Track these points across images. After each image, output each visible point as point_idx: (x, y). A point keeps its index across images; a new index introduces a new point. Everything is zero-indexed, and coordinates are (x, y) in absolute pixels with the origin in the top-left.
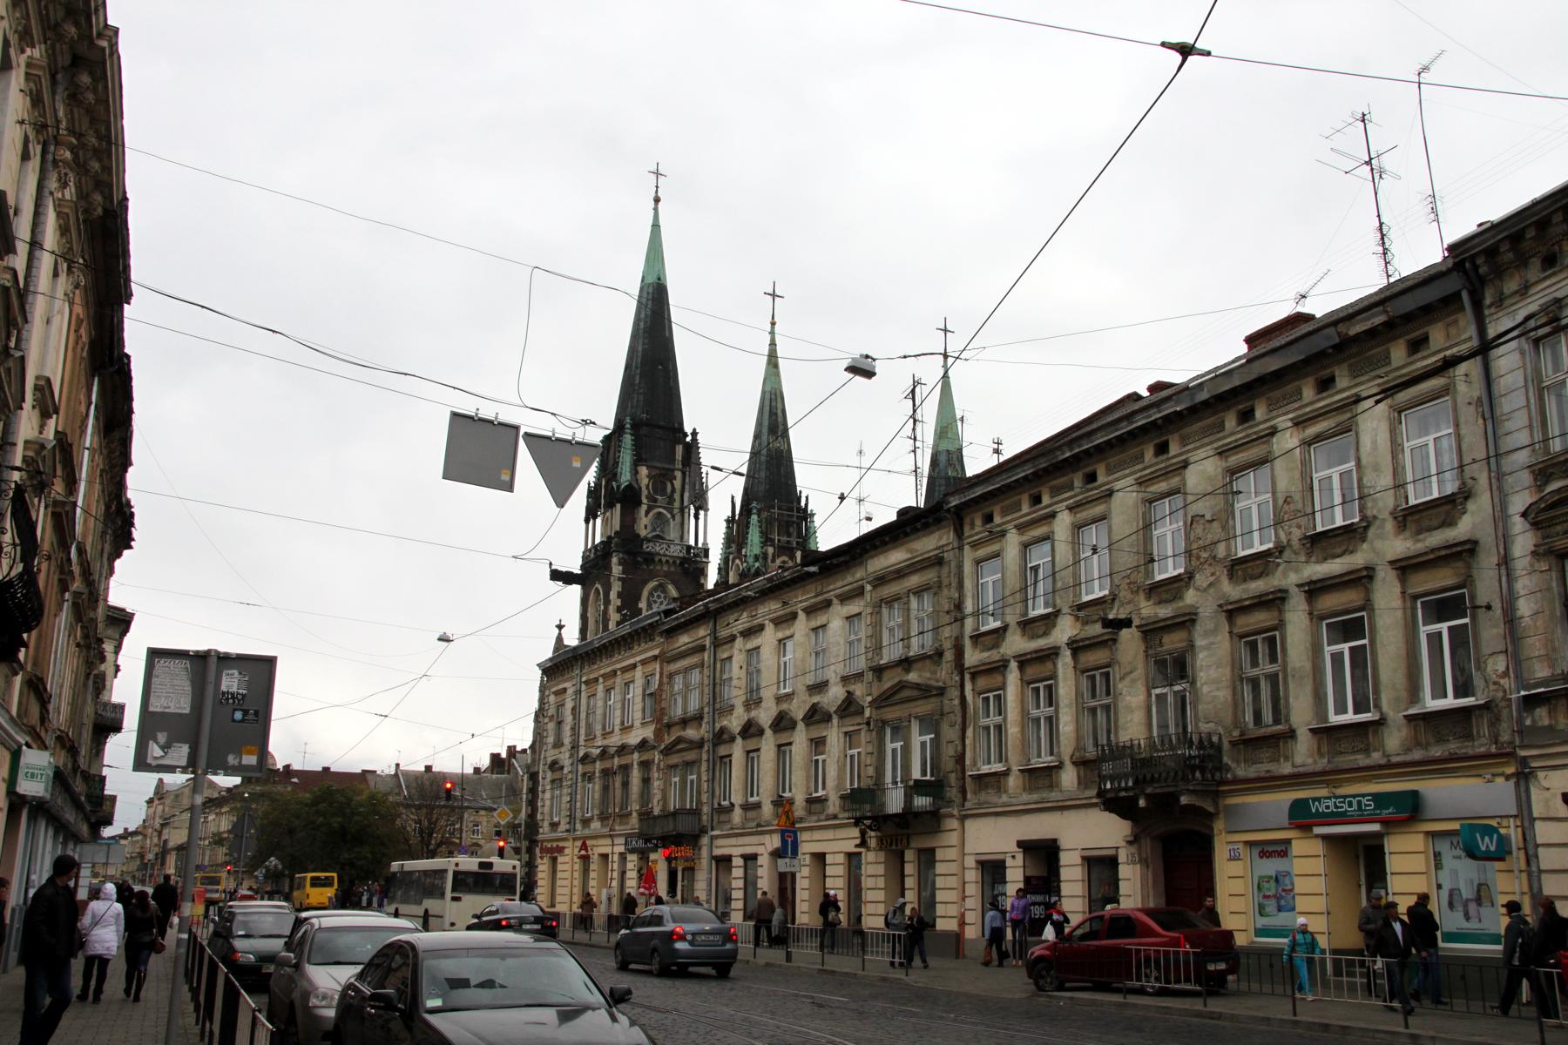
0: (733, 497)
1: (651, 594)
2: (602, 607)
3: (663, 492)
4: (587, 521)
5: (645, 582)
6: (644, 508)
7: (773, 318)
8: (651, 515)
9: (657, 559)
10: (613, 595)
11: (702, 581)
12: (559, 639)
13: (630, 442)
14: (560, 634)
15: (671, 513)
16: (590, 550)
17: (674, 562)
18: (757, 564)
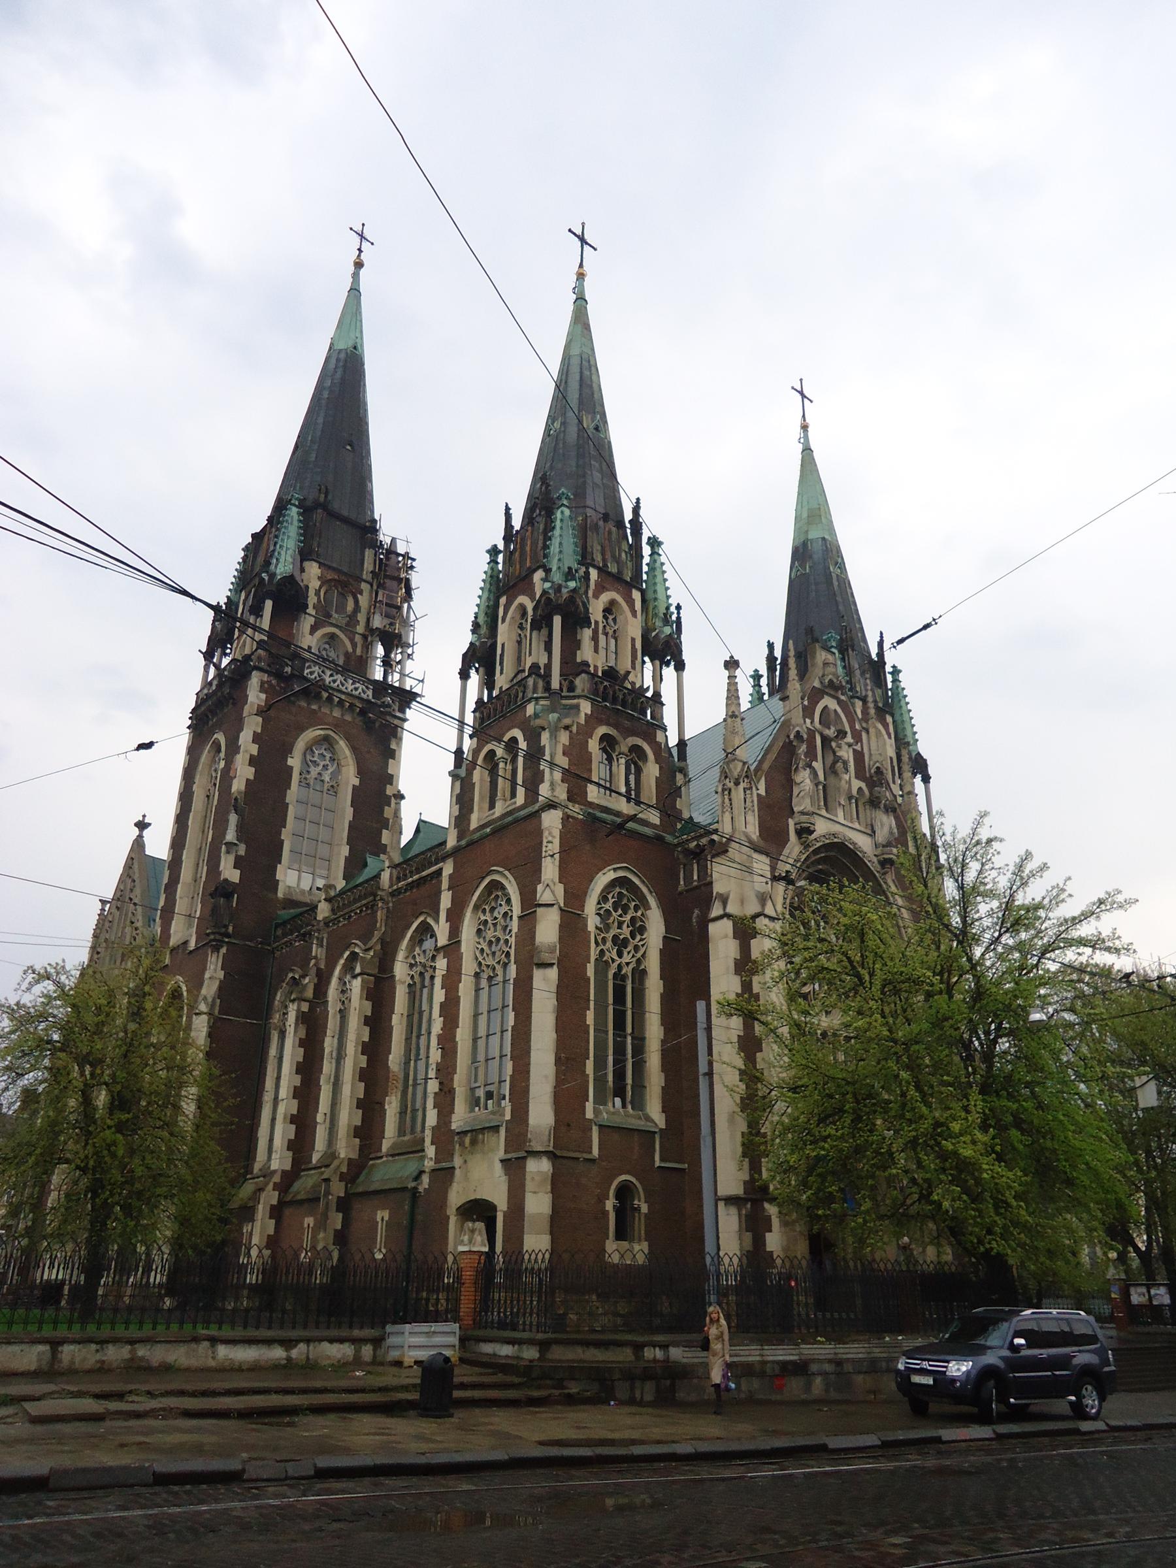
0: (507, 509)
1: (309, 749)
2: (222, 764)
3: (341, 608)
4: (208, 655)
5: (302, 729)
6: (312, 620)
7: (581, 266)
8: (319, 633)
9: (325, 695)
10: (245, 738)
11: (393, 746)
12: (139, 844)
13: (296, 523)
14: (140, 836)
15: (352, 641)
16: (210, 683)
17: (352, 705)
18: (572, 584)
